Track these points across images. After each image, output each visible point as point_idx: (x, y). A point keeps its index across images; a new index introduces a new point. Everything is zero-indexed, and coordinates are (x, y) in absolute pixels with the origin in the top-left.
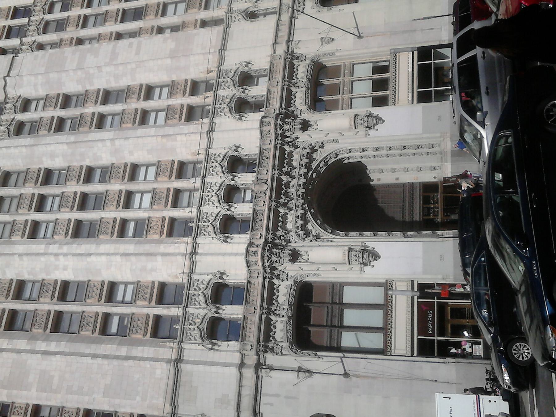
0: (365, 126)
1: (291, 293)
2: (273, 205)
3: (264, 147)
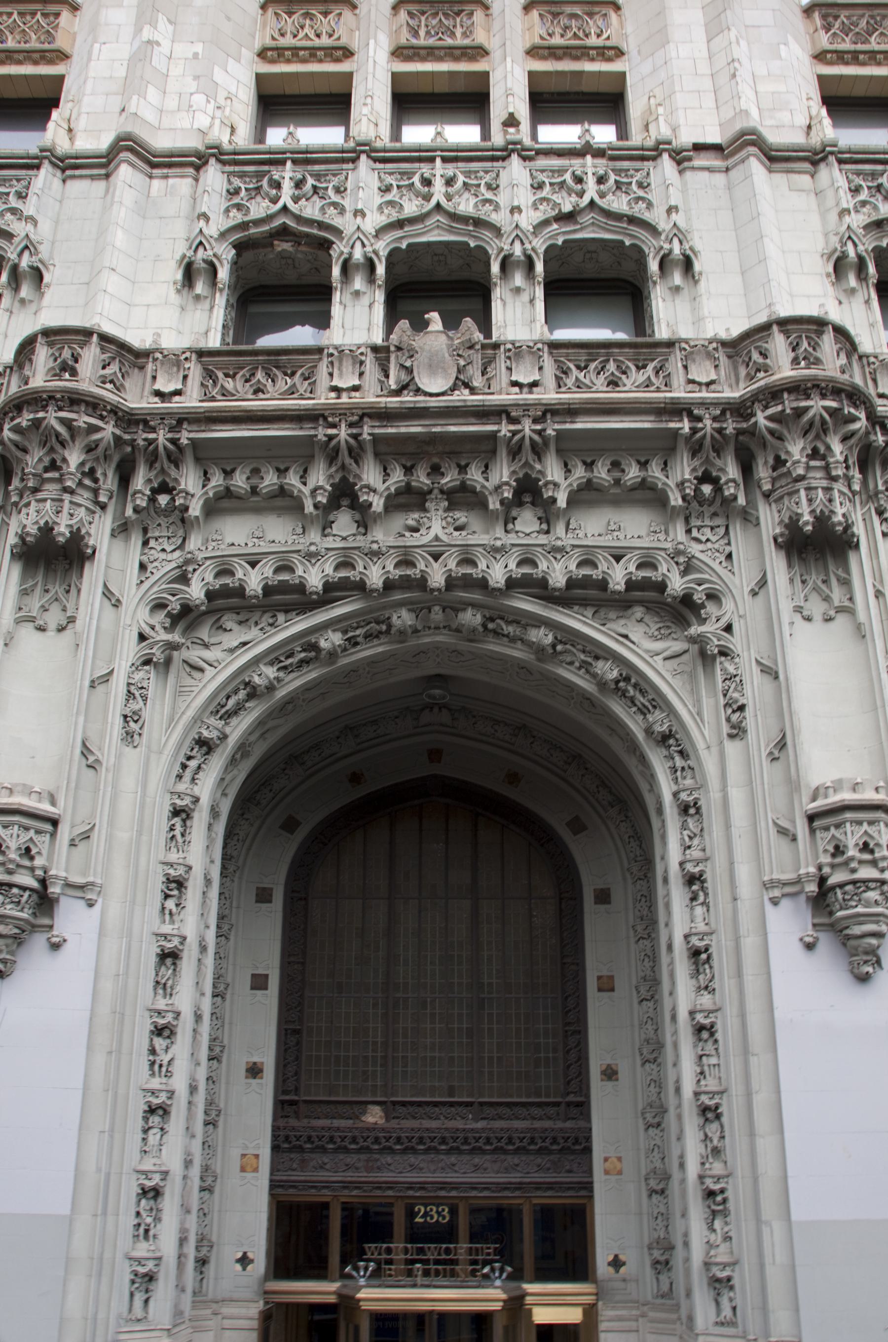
0: (826, 870)
3: (675, 364)
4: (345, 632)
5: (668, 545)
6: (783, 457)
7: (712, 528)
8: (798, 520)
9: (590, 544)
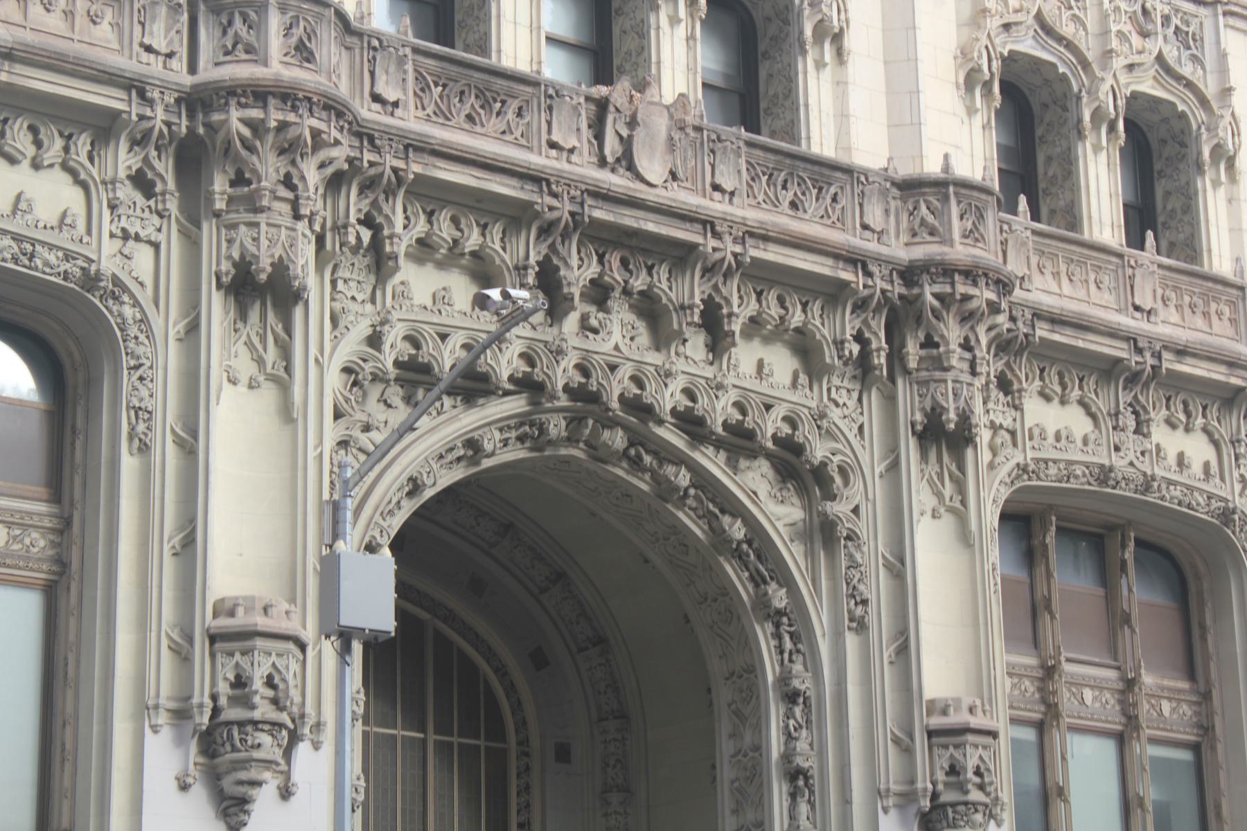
1: (38, 248)
2: (554, 203)
4: (501, 430)
5: (813, 404)
6: (936, 339)
7: (848, 391)
8: (941, 415)
9: (748, 387)
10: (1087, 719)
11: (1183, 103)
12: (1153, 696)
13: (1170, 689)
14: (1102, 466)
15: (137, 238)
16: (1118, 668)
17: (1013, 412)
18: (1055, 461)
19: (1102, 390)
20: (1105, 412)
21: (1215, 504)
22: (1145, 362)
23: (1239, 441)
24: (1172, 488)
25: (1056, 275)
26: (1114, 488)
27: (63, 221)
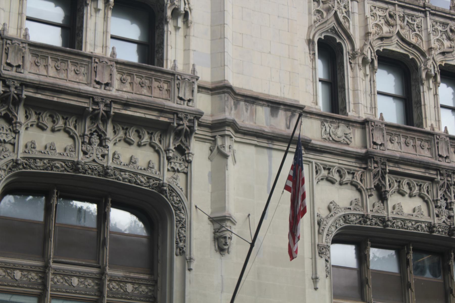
10: (72, 293)
11: (412, 54)
12: (121, 282)
13: (131, 278)
14: (73, 162)
15: (178, 171)
16: (99, 267)
17: (186, 165)
18: (41, 159)
19: (79, 124)
20: (163, 150)
21: (152, 182)
22: (100, 109)
23: (169, 150)
24: (122, 173)
25: (46, 66)
26: (85, 173)
27: (149, 166)
